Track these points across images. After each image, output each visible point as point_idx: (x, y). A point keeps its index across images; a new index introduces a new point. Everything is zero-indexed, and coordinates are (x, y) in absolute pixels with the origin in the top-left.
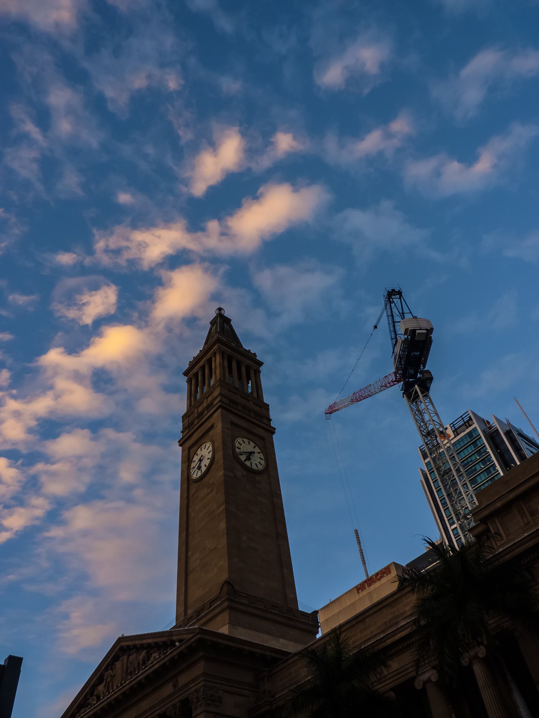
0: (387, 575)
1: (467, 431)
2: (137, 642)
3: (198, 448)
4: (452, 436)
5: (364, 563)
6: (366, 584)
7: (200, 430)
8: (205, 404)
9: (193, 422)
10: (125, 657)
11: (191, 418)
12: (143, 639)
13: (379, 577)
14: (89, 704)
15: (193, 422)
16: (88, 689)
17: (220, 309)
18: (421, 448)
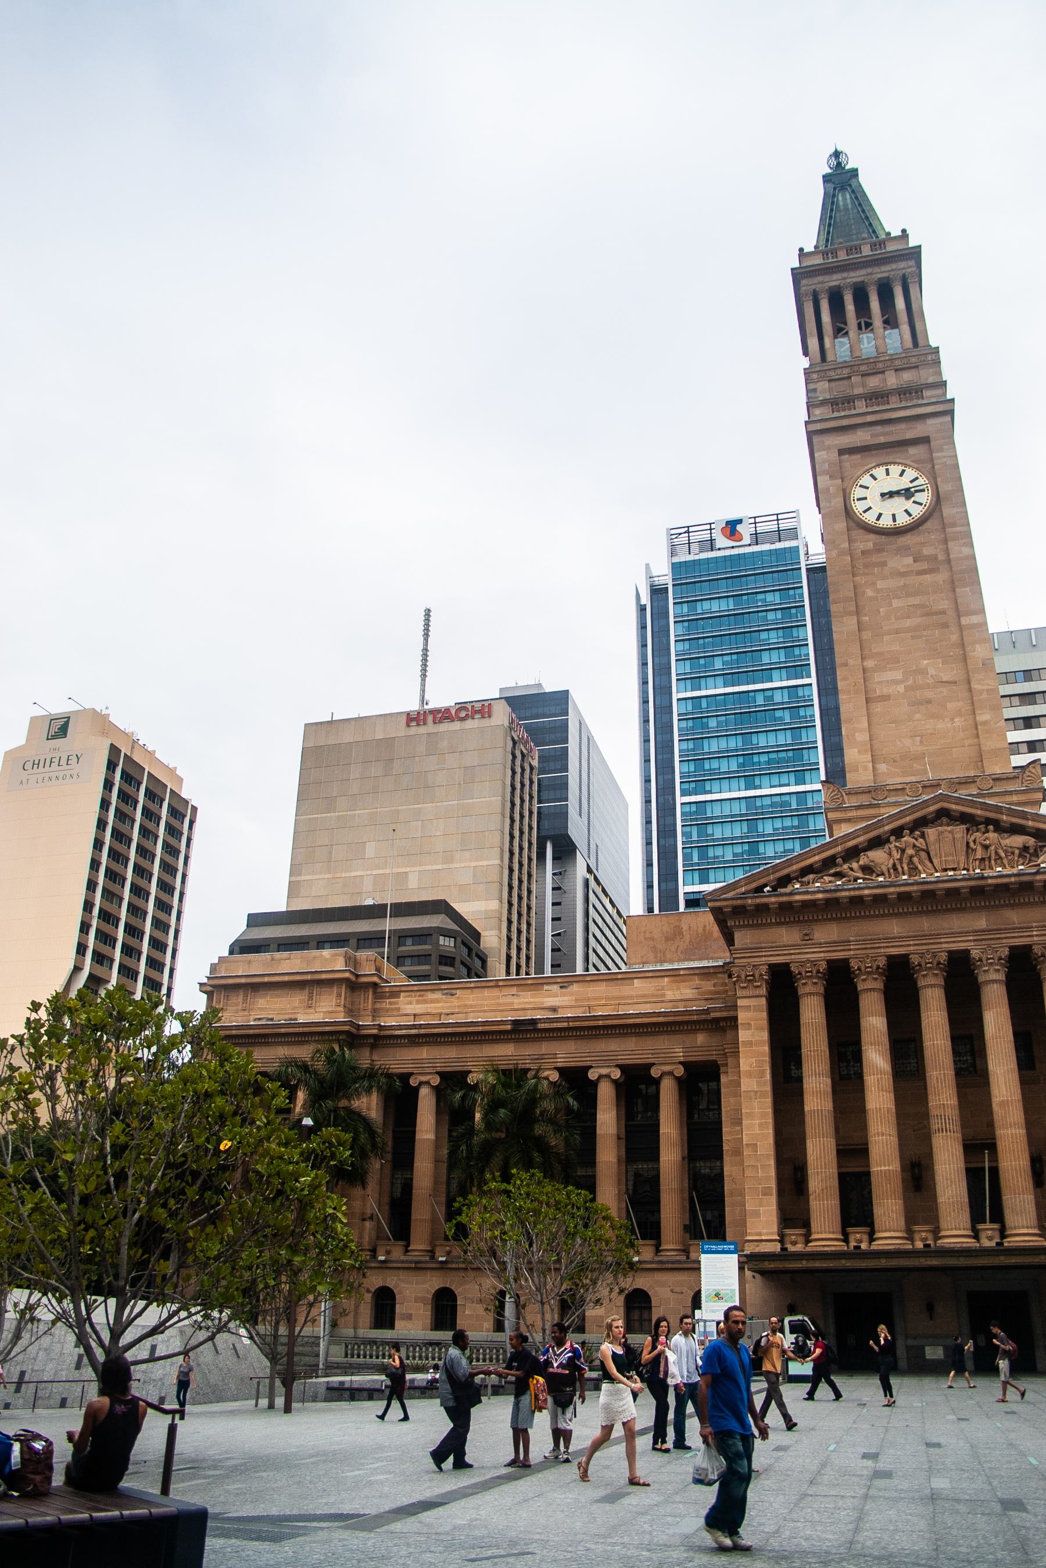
0: (483, 717)
1: (779, 545)
2: (1005, 817)
3: (878, 465)
4: (747, 540)
5: (424, 676)
6: (430, 718)
7: (879, 429)
8: (892, 381)
9: (849, 401)
10: (959, 830)
11: (840, 389)
12: (1027, 819)
13: (463, 714)
14: (839, 875)
15: (849, 401)
16: (839, 849)
17: (837, 154)
18: (673, 532)
